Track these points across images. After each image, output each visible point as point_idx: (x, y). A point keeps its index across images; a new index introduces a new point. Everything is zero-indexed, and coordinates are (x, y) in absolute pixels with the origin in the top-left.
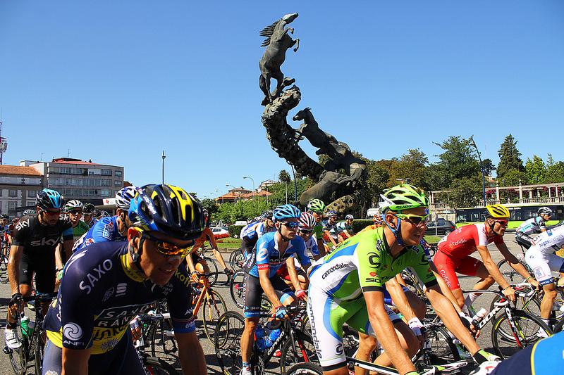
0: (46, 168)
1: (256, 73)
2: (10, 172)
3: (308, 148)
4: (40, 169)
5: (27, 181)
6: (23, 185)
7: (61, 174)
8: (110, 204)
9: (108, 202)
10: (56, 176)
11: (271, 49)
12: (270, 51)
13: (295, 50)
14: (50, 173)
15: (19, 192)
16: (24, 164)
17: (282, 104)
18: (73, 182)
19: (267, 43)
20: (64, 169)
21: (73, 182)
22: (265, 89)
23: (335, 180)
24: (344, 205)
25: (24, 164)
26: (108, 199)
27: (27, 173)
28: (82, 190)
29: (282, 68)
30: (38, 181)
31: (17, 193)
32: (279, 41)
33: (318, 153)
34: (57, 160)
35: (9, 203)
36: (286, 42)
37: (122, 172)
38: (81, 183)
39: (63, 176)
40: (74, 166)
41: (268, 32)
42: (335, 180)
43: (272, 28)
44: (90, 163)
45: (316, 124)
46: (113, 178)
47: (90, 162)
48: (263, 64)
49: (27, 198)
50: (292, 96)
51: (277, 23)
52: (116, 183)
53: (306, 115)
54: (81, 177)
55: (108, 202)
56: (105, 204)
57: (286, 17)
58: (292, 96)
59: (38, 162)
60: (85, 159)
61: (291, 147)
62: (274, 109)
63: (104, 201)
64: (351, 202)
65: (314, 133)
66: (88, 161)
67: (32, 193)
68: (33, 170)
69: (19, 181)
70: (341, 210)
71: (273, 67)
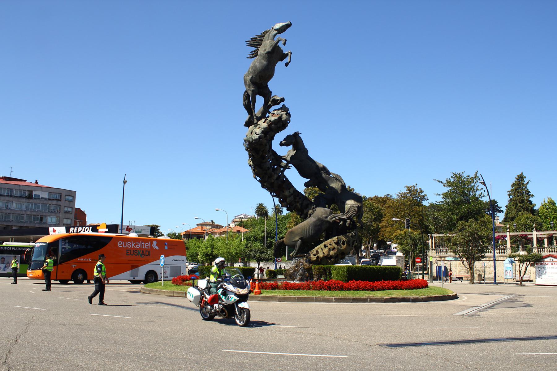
1: (240, 89)
9: (55, 231)
11: (258, 62)
12: (257, 64)
13: (287, 65)
18: (14, 205)
19: (254, 55)
21: (14, 205)
22: (249, 107)
23: (326, 217)
24: (336, 246)
26: (56, 228)
29: (271, 85)
32: (268, 53)
33: (306, 185)
36: (276, 55)
38: (24, 207)
40: (17, 188)
41: (256, 43)
42: (326, 217)
46: (62, 203)
47: (36, 182)
48: (249, 78)
50: (280, 118)
51: (266, 32)
52: (66, 209)
53: (294, 140)
54: (24, 200)
55: (55, 231)
57: (278, 26)
58: (280, 118)
60: (30, 180)
61: (276, 176)
62: (258, 131)
63: (51, 229)
64: (344, 244)
66: (34, 182)
70: (332, 253)
71: (259, 83)
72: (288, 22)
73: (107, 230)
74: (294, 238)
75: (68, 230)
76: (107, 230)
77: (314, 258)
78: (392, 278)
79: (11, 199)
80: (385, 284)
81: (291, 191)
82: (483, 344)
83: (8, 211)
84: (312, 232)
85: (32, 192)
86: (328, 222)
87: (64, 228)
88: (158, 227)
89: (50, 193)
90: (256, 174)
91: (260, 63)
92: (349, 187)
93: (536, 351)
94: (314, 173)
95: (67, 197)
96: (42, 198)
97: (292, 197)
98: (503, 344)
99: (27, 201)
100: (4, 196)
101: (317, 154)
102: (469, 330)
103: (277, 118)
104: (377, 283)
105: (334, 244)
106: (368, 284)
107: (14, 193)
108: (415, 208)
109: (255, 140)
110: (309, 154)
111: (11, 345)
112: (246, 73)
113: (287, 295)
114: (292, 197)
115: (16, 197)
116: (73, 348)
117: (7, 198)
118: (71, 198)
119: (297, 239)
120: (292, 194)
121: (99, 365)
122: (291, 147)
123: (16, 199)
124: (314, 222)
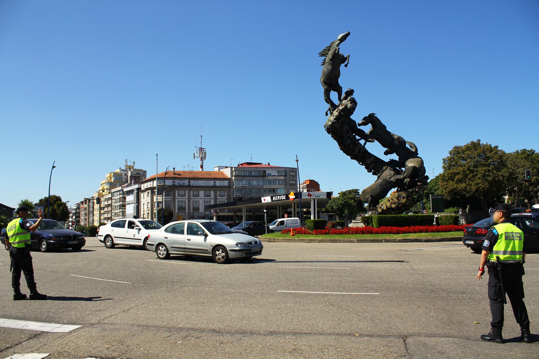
0: (232, 172)
1: (321, 89)
2: (204, 177)
3: (376, 149)
4: (227, 173)
5: (218, 183)
6: (214, 187)
7: (244, 176)
8: (266, 202)
9: (265, 200)
10: (241, 178)
11: (327, 67)
12: (325, 69)
13: (346, 66)
14: (235, 176)
15: (212, 193)
16: (216, 169)
17: (339, 113)
18: (255, 183)
19: (324, 63)
20: (250, 172)
21: (255, 183)
22: (328, 100)
23: (390, 178)
24: (396, 201)
25: (216, 169)
26: (265, 198)
27: (218, 177)
28: (262, 190)
29: (342, 81)
30: (226, 183)
31: (210, 193)
32: (331, 60)
33: (386, 153)
34: (242, 164)
35: (205, 202)
36: (338, 60)
37: (296, 173)
38: (261, 183)
39: (246, 178)
40: (255, 169)
41: (323, 54)
42: (390, 178)
43: (329, 49)
44: (267, 166)
45: (384, 127)
46: (288, 178)
47: (269, 165)
48: (322, 80)
49: (218, 197)
50: (346, 107)
51: (333, 43)
52: (291, 182)
53: (371, 119)
54: (261, 178)
55: (265, 200)
56: (263, 202)
57: (340, 37)
58: (346, 107)
59: (226, 167)
60: (265, 163)
61: (357, 150)
62: (332, 118)
63: (262, 199)
64: (404, 198)
65: (380, 133)
66: (267, 164)
67: (222, 193)
68: (222, 173)
69: (211, 183)
70: (393, 206)
71: (331, 82)
72: (347, 32)
73: (294, 197)
74: (366, 196)
75: (272, 198)
76: (294, 197)
77: (380, 210)
79: (252, 178)
80: (389, 228)
81: (372, 159)
83: (251, 187)
84: (378, 191)
85: (265, 172)
86: (391, 182)
87: (270, 197)
88: (358, 190)
89: (278, 171)
90: (341, 149)
91: (327, 68)
92: (490, 145)
94: (394, 144)
95: (291, 173)
96: (273, 176)
97: (374, 164)
99: (263, 178)
100: (247, 176)
101: (395, 129)
103: (343, 107)
104: (403, 229)
105: (395, 199)
106: (395, 229)
107: (253, 174)
109: (330, 126)
110: (388, 129)
112: (321, 77)
113: (325, 238)
114: (374, 164)
115: (255, 176)
117: (249, 178)
118: (294, 174)
119: (368, 196)
120: (373, 162)
122: (370, 125)
123: (255, 178)
124: (381, 183)
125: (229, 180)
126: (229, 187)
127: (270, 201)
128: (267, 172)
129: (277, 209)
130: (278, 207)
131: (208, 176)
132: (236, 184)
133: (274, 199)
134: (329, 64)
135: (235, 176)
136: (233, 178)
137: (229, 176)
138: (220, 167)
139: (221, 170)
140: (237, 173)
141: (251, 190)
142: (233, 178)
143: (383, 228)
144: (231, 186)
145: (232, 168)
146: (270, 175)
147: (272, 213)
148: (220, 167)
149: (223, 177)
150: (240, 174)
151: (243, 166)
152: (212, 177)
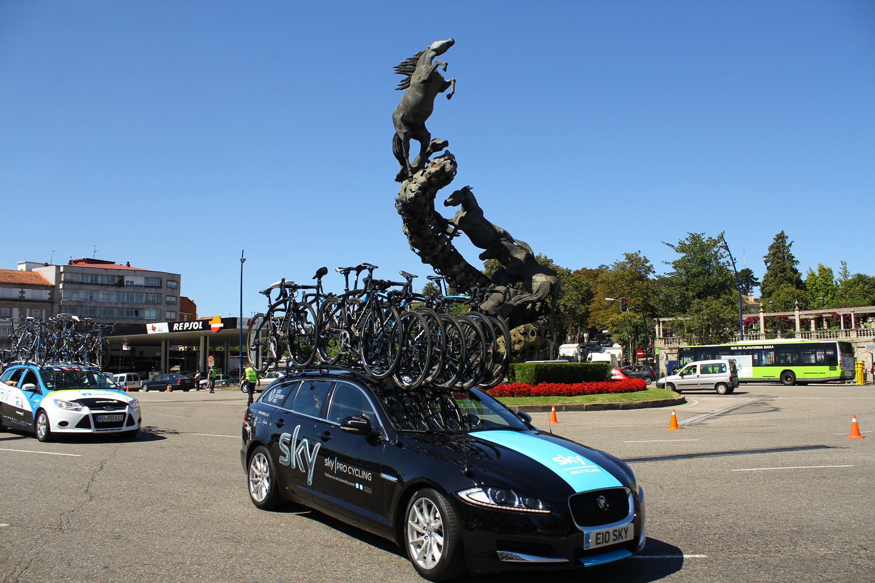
0: (58, 274)
1: (390, 132)
4: (49, 276)
5: (29, 294)
6: (22, 300)
7: (82, 283)
8: (157, 332)
9: (154, 329)
10: (76, 286)
11: (411, 95)
12: (410, 98)
13: (449, 97)
14: (65, 282)
15: (16, 312)
16: (23, 267)
18: (101, 296)
19: (405, 85)
20: (86, 274)
21: (101, 296)
22: (401, 154)
25: (23, 267)
26: (155, 325)
27: (29, 282)
28: (115, 311)
29: (430, 124)
30: (45, 295)
31: (11, 312)
32: (424, 82)
33: (482, 257)
34: (76, 262)
36: (435, 84)
38: (114, 298)
39: (85, 287)
40: (104, 272)
41: (407, 68)
47: (128, 265)
48: (399, 117)
51: (420, 54)
52: (168, 299)
53: (464, 197)
54: (113, 289)
55: (154, 329)
56: (150, 331)
57: (436, 45)
59: (47, 265)
60: (120, 262)
61: (440, 247)
62: (414, 187)
63: (149, 326)
64: (533, 334)
66: (125, 264)
68: (37, 276)
69: (15, 293)
71: (414, 123)
72: (450, 40)
73: (222, 325)
75: (171, 327)
76: (222, 325)
78: (593, 377)
79: (96, 288)
80: (586, 386)
81: (462, 265)
82: (694, 460)
83: (93, 305)
85: (122, 277)
86: (511, 305)
89: (146, 278)
90: (414, 245)
92: (546, 257)
93: (759, 466)
94: (492, 240)
95: (169, 283)
96: (137, 286)
97: (463, 274)
98: (720, 458)
99: (118, 289)
101: (495, 215)
102: (682, 442)
103: (438, 168)
104: (576, 386)
105: (520, 336)
107: (99, 281)
108: (383, 296)
109: (410, 199)
111: (95, 472)
112: (396, 110)
114: (463, 274)
115: (102, 285)
116: (170, 474)
117: (91, 287)
118: (174, 284)
120: (462, 271)
121: (199, 493)
123: (103, 288)
125: (52, 288)
126: (51, 302)
127: (167, 331)
128: (126, 279)
129: (160, 345)
130: (163, 343)
131: (9, 280)
132: (64, 296)
133: (176, 327)
134: (418, 88)
135: (65, 282)
136: (61, 286)
137: (53, 283)
138: (30, 265)
139: (34, 270)
140: (69, 277)
141: (93, 310)
142: (61, 286)
143: (543, 386)
144: (56, 300)
145: (58, 267)
146: (132, 285)
147: (142, 353)
148: (30, 265)
149: (39, 283)
150: (75, 278)
151: (79, 265)
152: (17, 281)
